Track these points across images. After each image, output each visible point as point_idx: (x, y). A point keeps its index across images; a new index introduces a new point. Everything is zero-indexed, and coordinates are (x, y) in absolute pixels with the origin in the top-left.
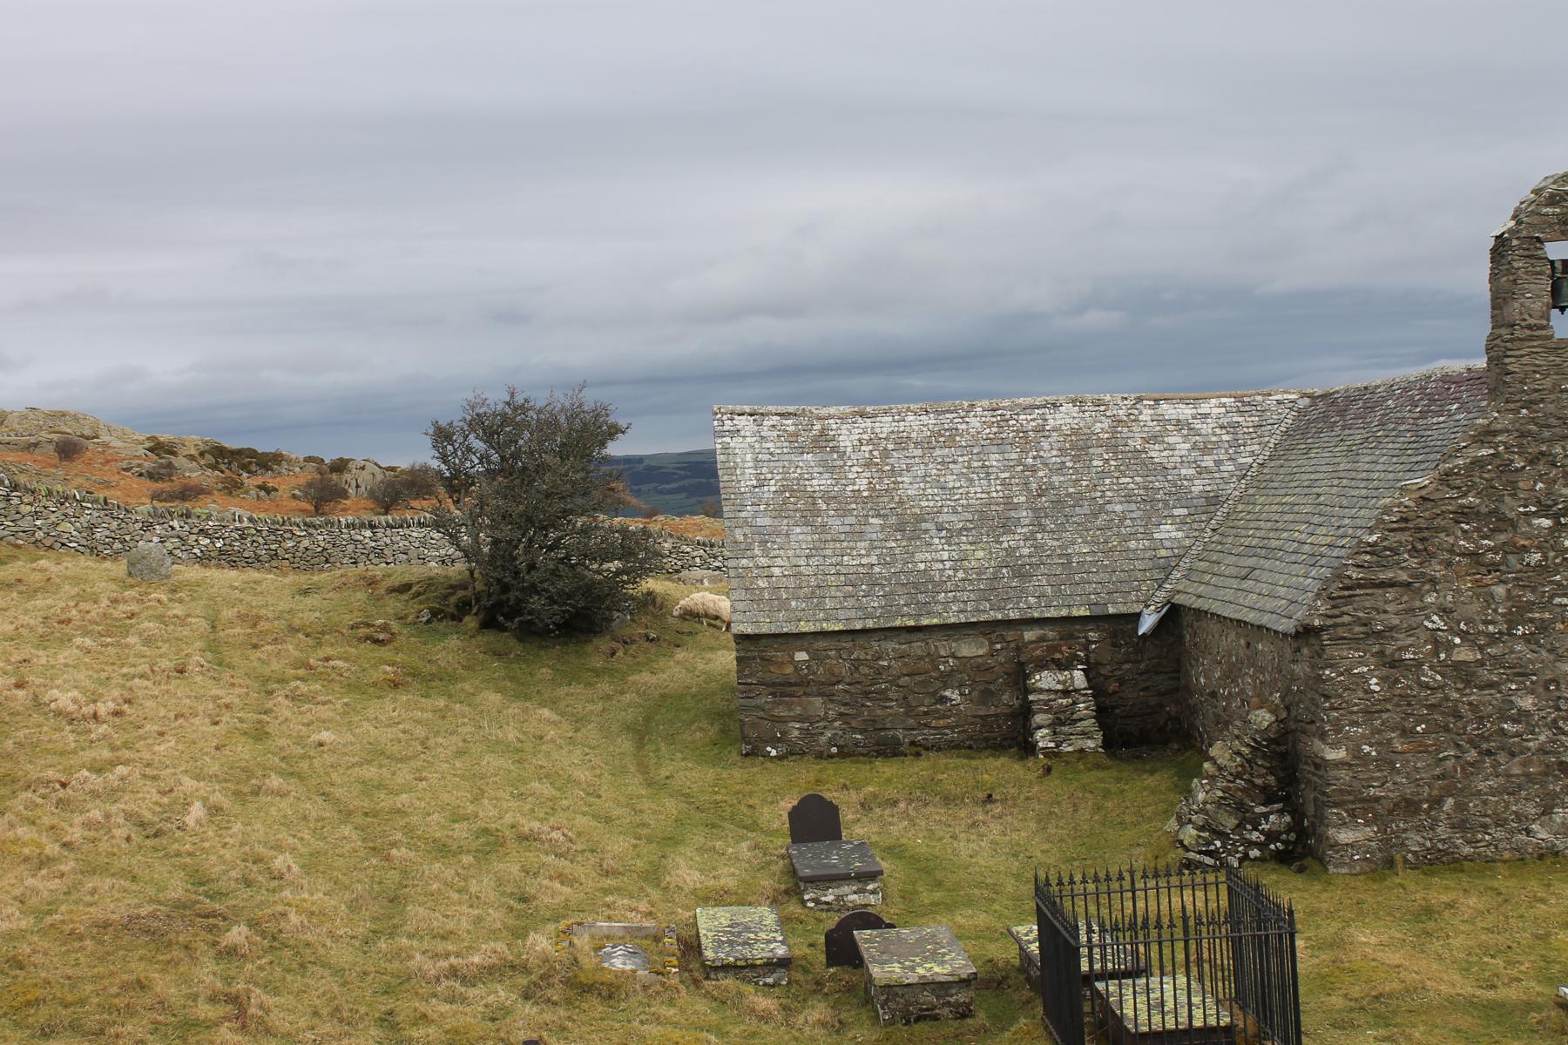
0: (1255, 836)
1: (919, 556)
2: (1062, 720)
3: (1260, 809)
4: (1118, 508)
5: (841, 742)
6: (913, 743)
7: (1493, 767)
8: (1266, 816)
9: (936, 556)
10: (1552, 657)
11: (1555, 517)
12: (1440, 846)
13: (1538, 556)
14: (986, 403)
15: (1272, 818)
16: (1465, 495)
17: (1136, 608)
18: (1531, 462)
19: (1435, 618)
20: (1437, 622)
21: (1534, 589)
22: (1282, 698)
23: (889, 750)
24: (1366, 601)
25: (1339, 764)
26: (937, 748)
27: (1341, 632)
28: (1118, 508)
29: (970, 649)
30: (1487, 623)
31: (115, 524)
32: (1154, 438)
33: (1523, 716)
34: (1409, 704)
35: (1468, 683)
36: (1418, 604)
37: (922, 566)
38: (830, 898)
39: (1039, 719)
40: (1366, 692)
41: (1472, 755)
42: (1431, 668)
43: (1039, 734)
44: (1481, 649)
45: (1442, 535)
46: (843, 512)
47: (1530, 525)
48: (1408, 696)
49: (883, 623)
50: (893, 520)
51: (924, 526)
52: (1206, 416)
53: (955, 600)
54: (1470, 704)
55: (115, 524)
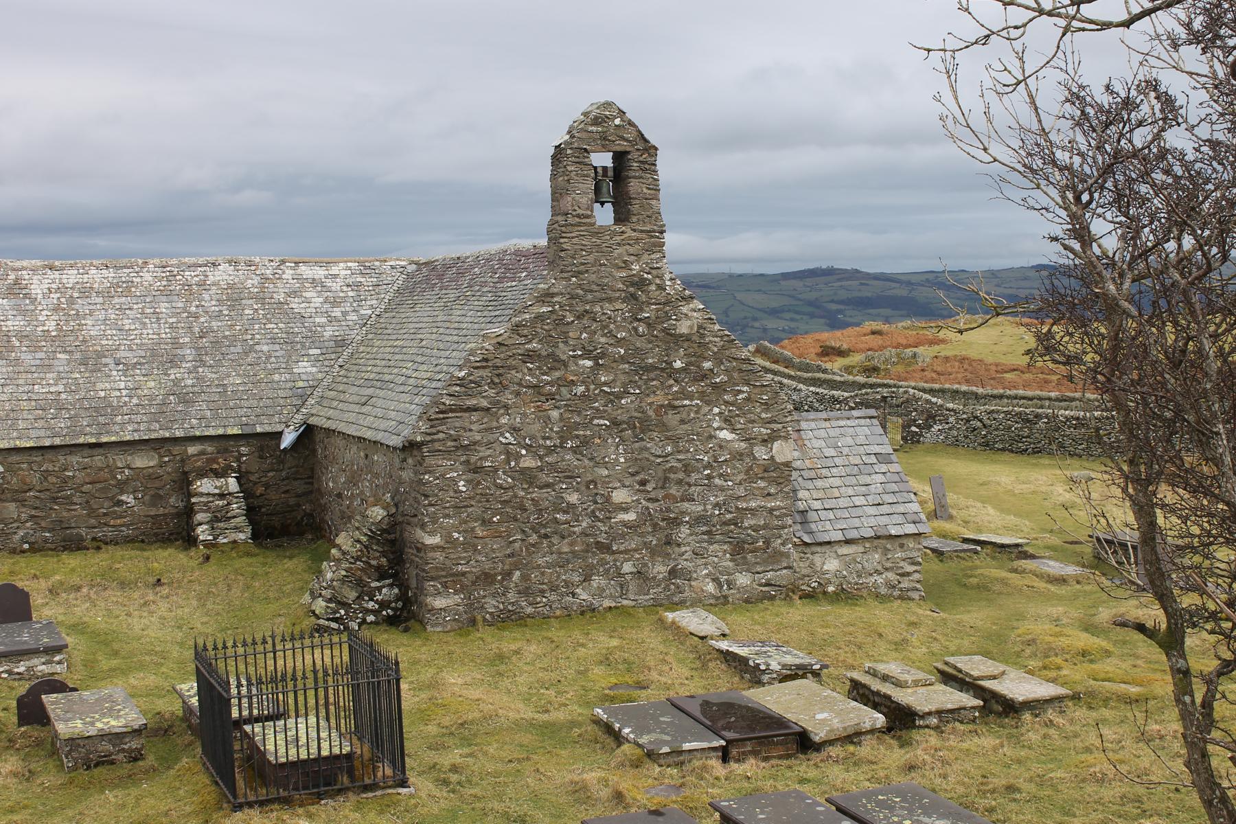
0: (371, 605)
1: (100, 386)
2: (219, 517)
3: (375, 584)
4: (265, 348)
5: (32, 539)
6: (94, 539)
7: (549, 547)
8: (379, 589)
9: (113, 386)
10: (591, 464)
11: (595, 359)
12: (510, 607)
13: (582, 388)
14: (157, 261)
15: (384, 591)
16: (530, 342)
17: (279, 428)
18: (578, 318)
19: (507, 435)
21: (579, 413)
22: (393, 499)
23: (73, 545)
24: (456, 421)
25: (434, 548)
26: (116, 543)
27: (437, 446)
28: (265, 348)
29: (143, 461)
30: (544, 438)
32: (294, 293)
33: (571, 507)
34: (488, 501)
35: (531, 484)
36: (495, 424)
37: (102, 394)
38: (21, 669)
39: (200, 517)
40: (456, 492)
41: (534, 538)
42: (504, 473)
43: (200, 529)
44: (541, 458)
45: (513, 372)
46: (35, 349)
47: (577, 365)
48: (486, 494)
49: (68, 441)
50: (78, 356)
51: (104, 360)
52: (335, 276)
53: (130, 421)
54: (533, 500)
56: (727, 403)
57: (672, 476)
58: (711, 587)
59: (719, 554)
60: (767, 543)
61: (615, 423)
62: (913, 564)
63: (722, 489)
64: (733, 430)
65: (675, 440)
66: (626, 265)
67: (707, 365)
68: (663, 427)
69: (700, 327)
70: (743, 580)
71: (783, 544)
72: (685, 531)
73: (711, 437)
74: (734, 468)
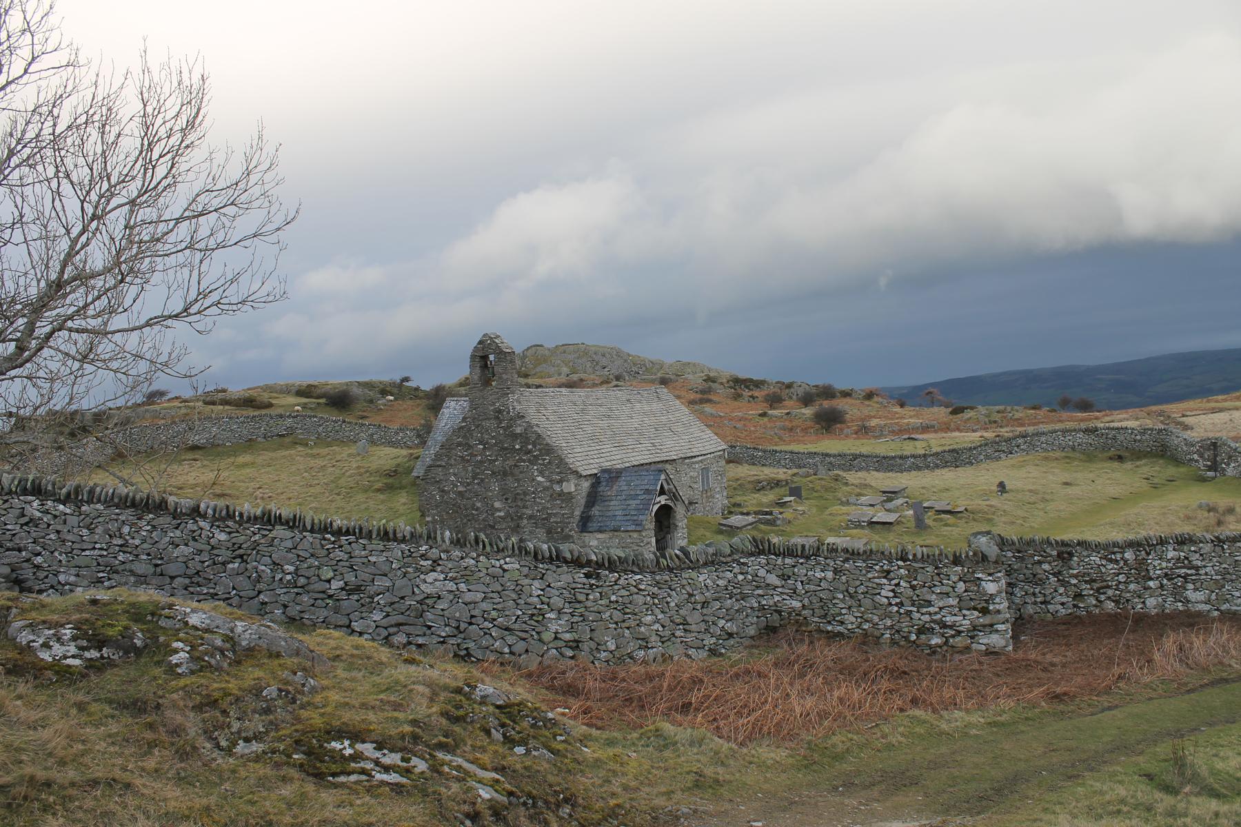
20: (453, 478)
59: (541, 533)
61: (494, 473)
65: (518, 480)
66: (494, 404)
68: (512, 474)
72: (525, 521)
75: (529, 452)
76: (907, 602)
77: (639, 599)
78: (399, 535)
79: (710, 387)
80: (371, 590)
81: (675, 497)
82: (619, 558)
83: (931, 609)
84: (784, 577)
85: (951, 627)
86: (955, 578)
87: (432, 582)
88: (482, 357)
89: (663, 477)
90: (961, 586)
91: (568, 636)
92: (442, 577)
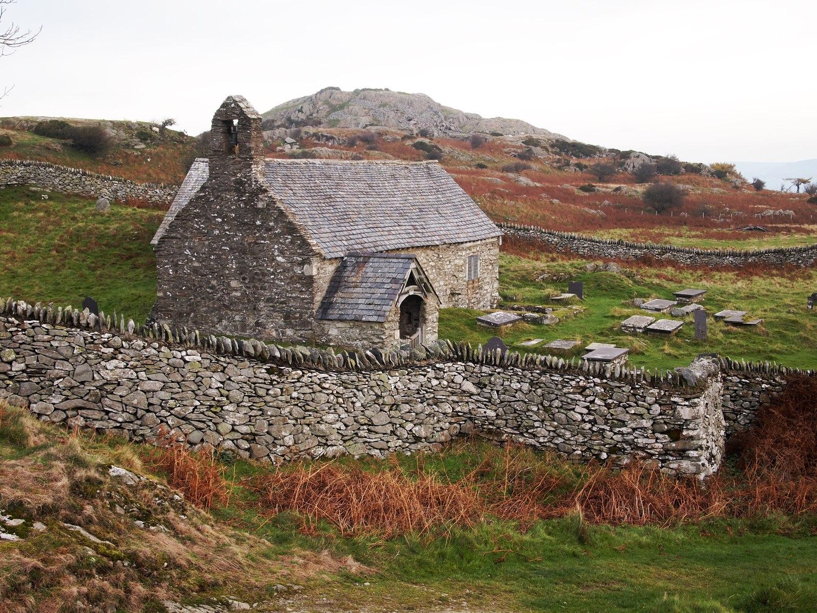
20: (188, 252)
31: (128, 190)
33: (213, 287)
55: (128, 190)
56: (281, 243)
57: (256, 277)
58: (274, 334)
60: (301, 316)
62: (378, 338)
63: (279, 286)
64: (284, 257)
67: (272, 224)
69: (267, 205)
70: (289, 332)
71: (309, 317)
73: (274, 260)
74: (285, 276)
75: (269, 229)
76: (600, 420)
77: (322, 397)
78: (83, 322)
79: (530, 150)
80: (53, 373)
81: (427, 287)
82: (304, 356)
83: (624, 429)
84: (480, 385)
85: (643, 449)
86: (650, 399)
87: (113, 369)
88: (224, 122)
89: (413, 265)
90: (656, 409)
91: (244, 429)
92: (122, 364)
